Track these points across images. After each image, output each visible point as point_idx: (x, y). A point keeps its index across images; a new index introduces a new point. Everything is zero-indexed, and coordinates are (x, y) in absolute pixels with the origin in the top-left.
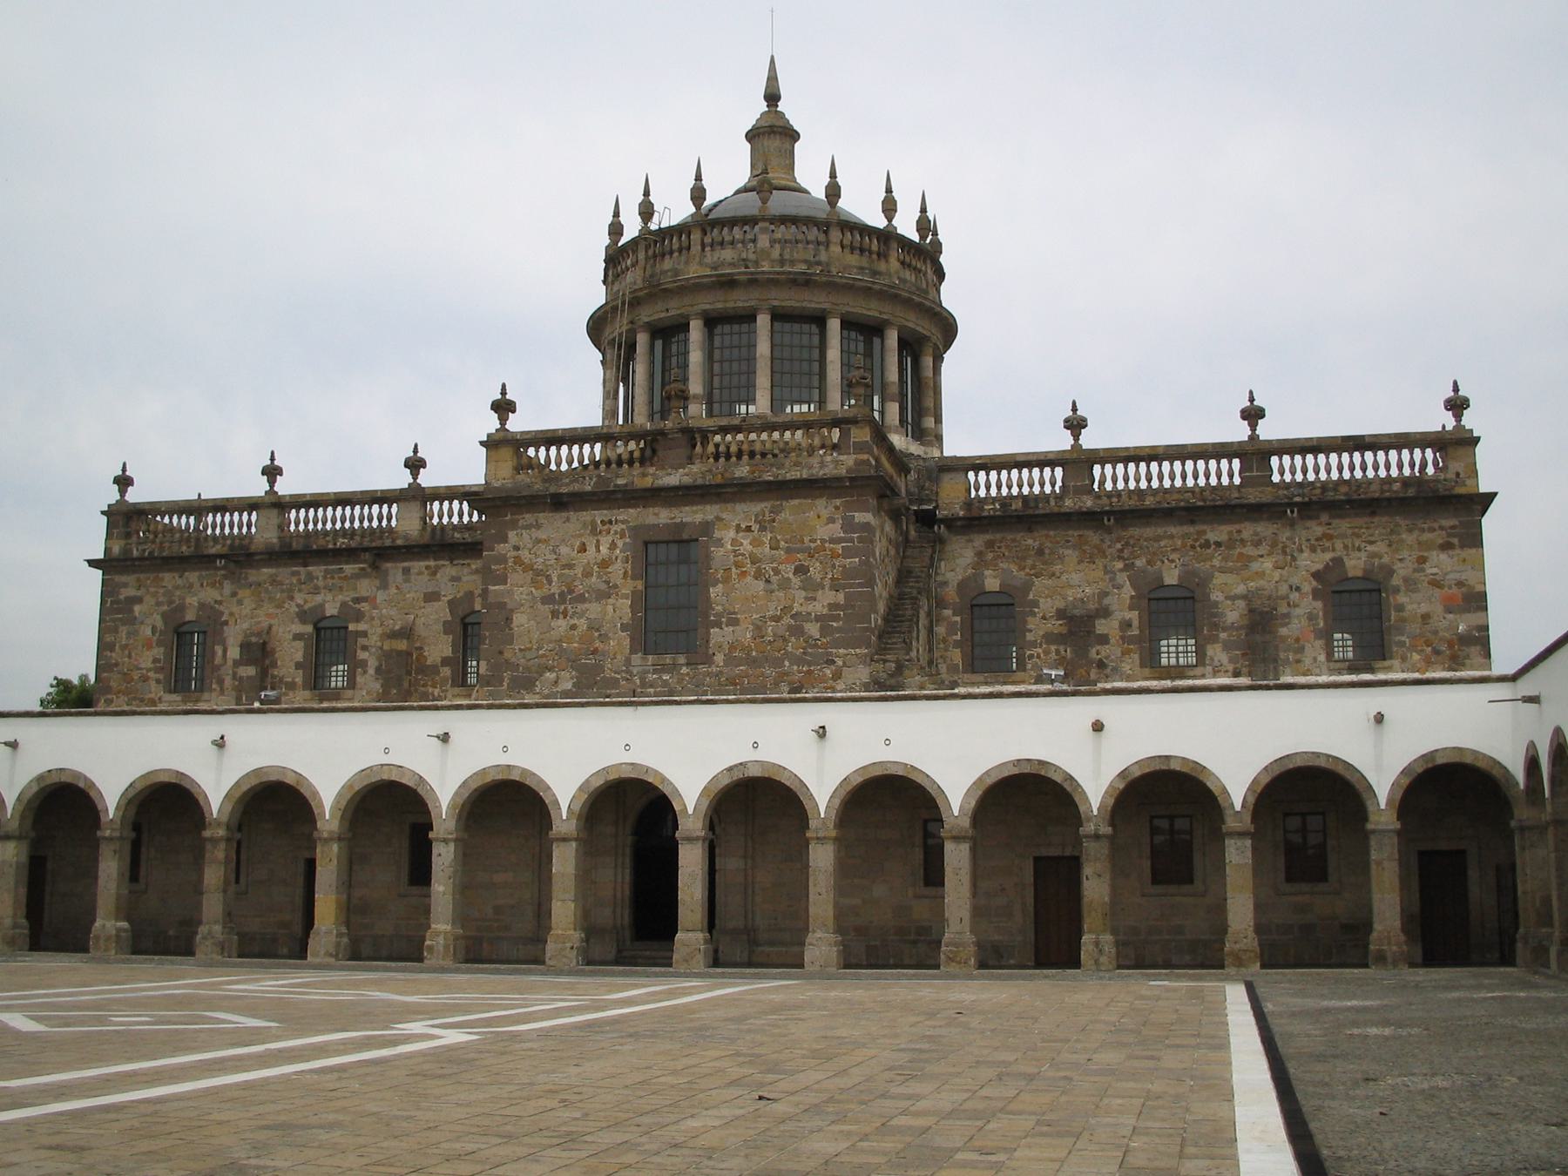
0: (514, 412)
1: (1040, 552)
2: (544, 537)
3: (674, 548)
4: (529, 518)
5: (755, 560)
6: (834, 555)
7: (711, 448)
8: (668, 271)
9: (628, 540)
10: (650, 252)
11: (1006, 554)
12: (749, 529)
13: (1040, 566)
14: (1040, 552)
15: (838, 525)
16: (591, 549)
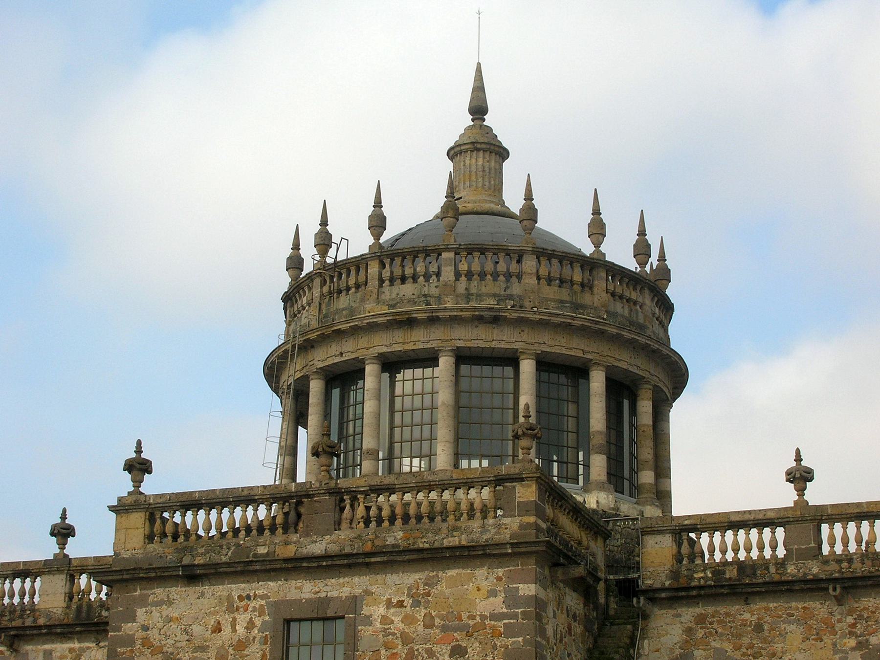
0: (150, 472)
1: (759, 628)
2: (176, 615)
3: (318, 626)
4: (159, 592)
5: (406, 639)
6: (496, 634)
7: (360, 511)
8: (343, 309)
9: (267, 618)
10: (326, 289)
11: (720, 630)
12: (400, 604)
13: (758, 644)
14: (759, 628)
15: (500, 598)
16: (227, 630)
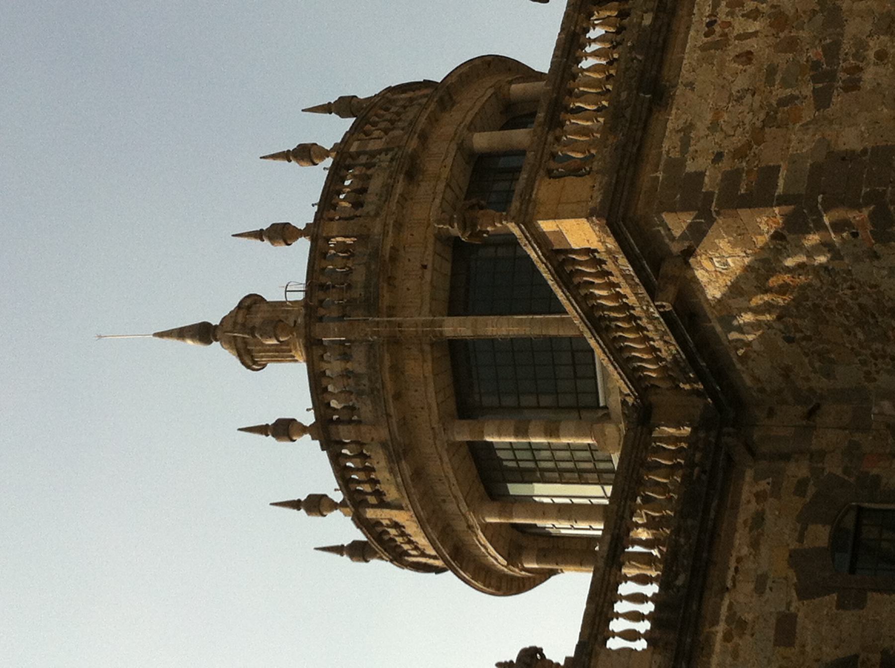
16: (752, 44)
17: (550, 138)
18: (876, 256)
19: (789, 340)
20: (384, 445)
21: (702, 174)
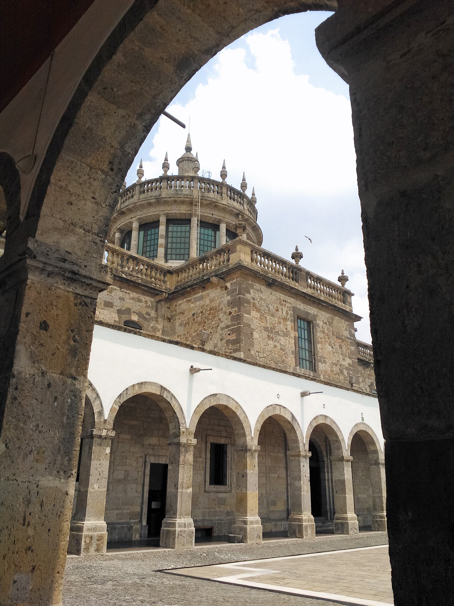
17: (261, 253)
18: (221, 340)
19: (193, 315)
20: (160, 195)
21: (250, 294)
